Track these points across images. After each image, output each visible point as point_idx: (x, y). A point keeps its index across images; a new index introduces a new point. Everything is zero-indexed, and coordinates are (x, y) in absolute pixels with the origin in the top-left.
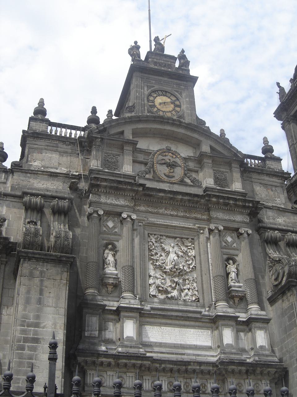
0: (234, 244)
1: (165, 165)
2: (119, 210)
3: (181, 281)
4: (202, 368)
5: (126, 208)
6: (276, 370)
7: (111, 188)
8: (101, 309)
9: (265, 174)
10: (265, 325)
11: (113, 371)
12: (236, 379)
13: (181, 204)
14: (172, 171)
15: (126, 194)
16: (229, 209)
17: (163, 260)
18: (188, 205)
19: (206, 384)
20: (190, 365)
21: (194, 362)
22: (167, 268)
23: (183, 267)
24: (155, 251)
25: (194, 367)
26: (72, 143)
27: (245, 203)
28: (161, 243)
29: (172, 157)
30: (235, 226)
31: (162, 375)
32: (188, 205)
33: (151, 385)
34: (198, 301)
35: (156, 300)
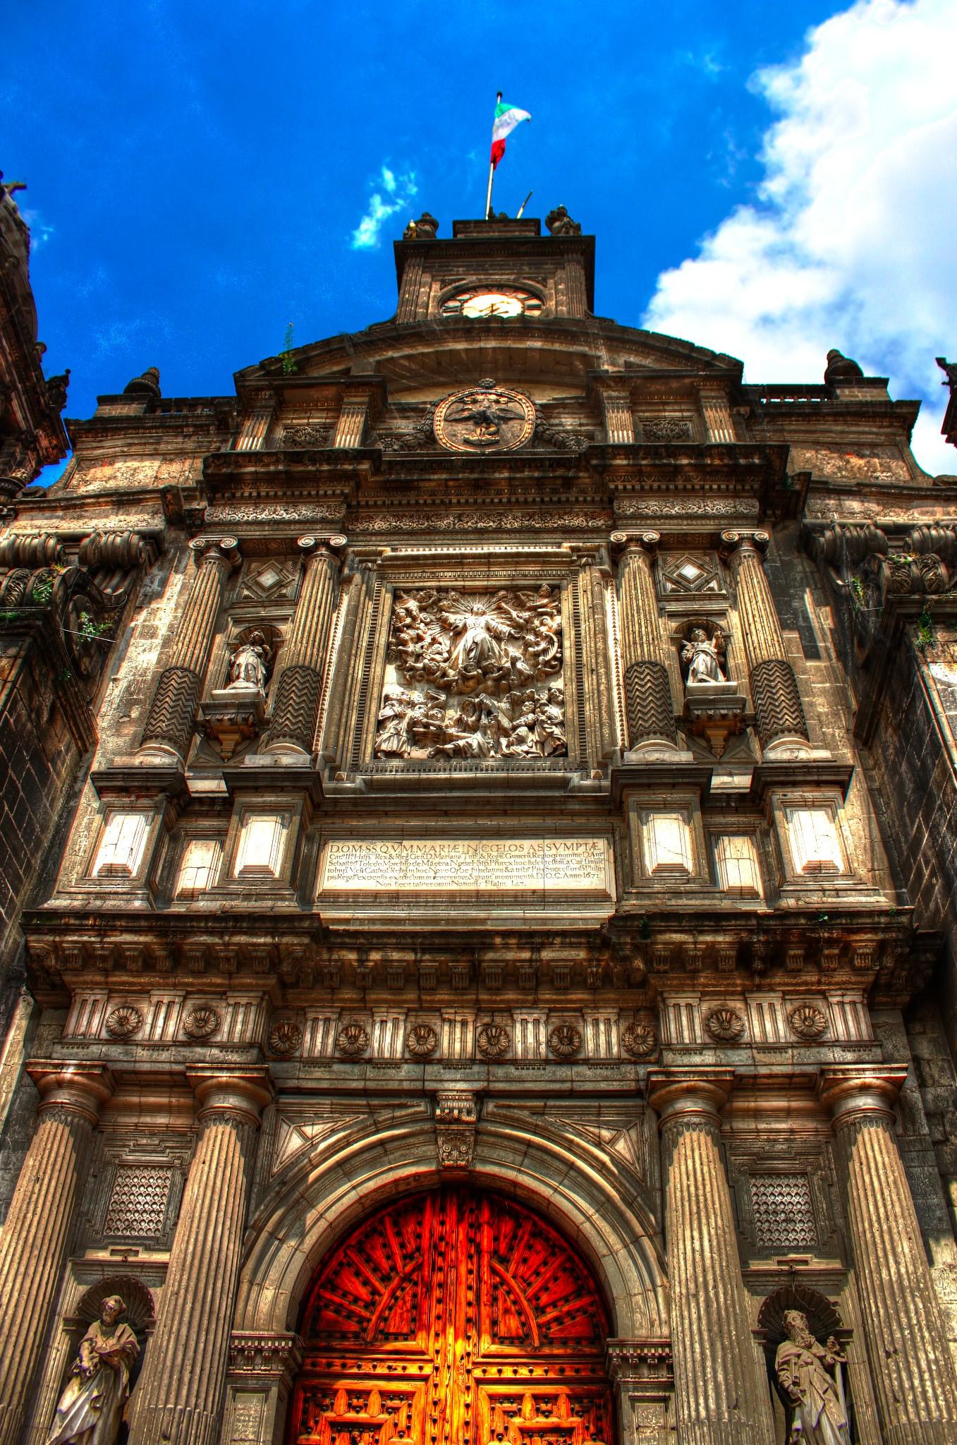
0: (708, 582)
1: (471, 422)
2: (290, 532)
3: (504, 705)
4: (546, 955)
5: (318, 527)
6: (880, 936)
7: (271, 478)
8: (163, 790)
9: (829, 415)
10: (833, 793)
11: (175, 986)
12: (704, 994)
13: (513, 499)
14: (492, 429)
15: (321, 492)
16: (681, 487)
17: (440, 654)
18: (538, 499)
19: (580, 1029)
20: (492, 947)
21: (506, 934)
22: (451, 672)
23: (513, 664)
24: (412, 633)
25: (510, 956)
26: (201, 426)
27: (737, 459)
28: (441, 610)
29: (497, 402)
30: (708, 527)
31: (385, 1001)
32: (538, 499)
33: (336, 1040)
34: (565, 755)
35: (395, 763)
